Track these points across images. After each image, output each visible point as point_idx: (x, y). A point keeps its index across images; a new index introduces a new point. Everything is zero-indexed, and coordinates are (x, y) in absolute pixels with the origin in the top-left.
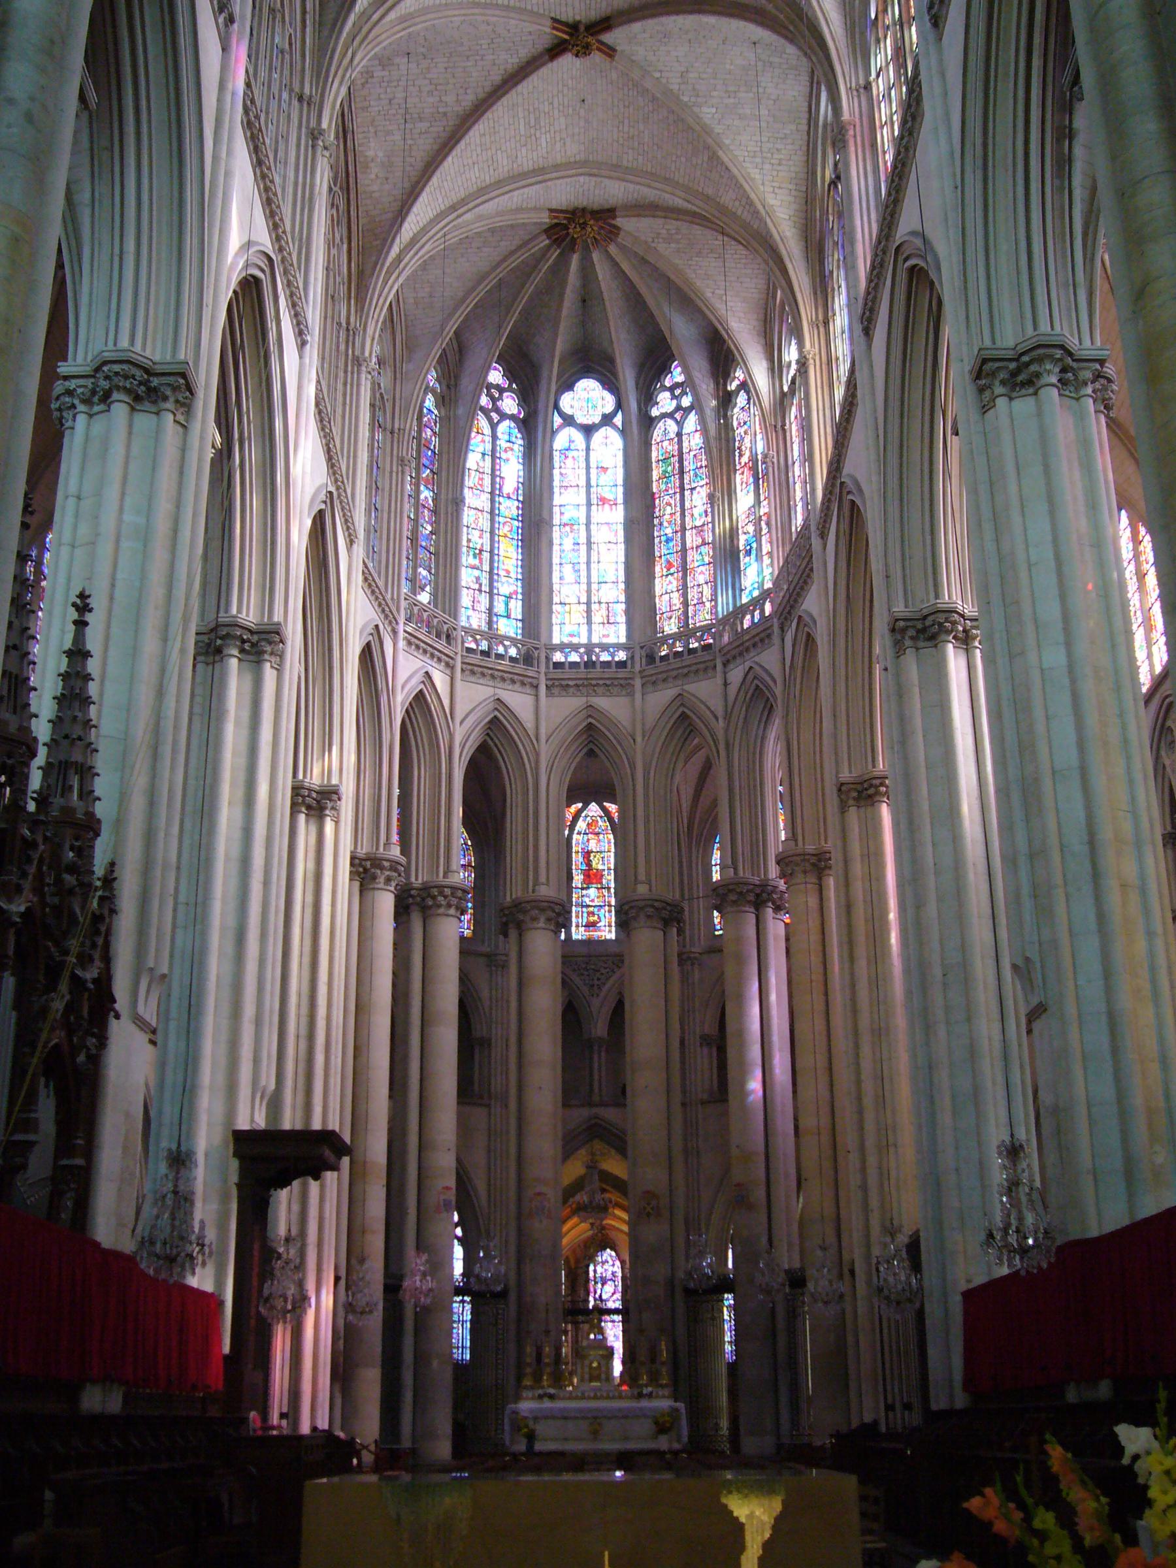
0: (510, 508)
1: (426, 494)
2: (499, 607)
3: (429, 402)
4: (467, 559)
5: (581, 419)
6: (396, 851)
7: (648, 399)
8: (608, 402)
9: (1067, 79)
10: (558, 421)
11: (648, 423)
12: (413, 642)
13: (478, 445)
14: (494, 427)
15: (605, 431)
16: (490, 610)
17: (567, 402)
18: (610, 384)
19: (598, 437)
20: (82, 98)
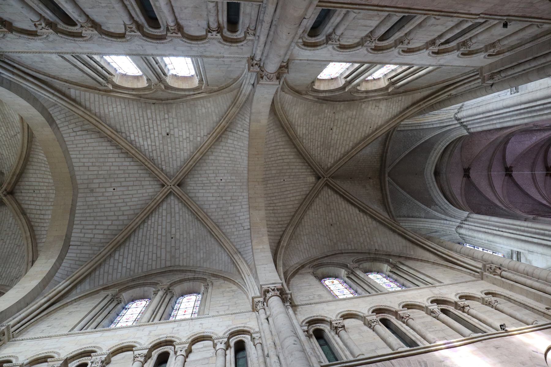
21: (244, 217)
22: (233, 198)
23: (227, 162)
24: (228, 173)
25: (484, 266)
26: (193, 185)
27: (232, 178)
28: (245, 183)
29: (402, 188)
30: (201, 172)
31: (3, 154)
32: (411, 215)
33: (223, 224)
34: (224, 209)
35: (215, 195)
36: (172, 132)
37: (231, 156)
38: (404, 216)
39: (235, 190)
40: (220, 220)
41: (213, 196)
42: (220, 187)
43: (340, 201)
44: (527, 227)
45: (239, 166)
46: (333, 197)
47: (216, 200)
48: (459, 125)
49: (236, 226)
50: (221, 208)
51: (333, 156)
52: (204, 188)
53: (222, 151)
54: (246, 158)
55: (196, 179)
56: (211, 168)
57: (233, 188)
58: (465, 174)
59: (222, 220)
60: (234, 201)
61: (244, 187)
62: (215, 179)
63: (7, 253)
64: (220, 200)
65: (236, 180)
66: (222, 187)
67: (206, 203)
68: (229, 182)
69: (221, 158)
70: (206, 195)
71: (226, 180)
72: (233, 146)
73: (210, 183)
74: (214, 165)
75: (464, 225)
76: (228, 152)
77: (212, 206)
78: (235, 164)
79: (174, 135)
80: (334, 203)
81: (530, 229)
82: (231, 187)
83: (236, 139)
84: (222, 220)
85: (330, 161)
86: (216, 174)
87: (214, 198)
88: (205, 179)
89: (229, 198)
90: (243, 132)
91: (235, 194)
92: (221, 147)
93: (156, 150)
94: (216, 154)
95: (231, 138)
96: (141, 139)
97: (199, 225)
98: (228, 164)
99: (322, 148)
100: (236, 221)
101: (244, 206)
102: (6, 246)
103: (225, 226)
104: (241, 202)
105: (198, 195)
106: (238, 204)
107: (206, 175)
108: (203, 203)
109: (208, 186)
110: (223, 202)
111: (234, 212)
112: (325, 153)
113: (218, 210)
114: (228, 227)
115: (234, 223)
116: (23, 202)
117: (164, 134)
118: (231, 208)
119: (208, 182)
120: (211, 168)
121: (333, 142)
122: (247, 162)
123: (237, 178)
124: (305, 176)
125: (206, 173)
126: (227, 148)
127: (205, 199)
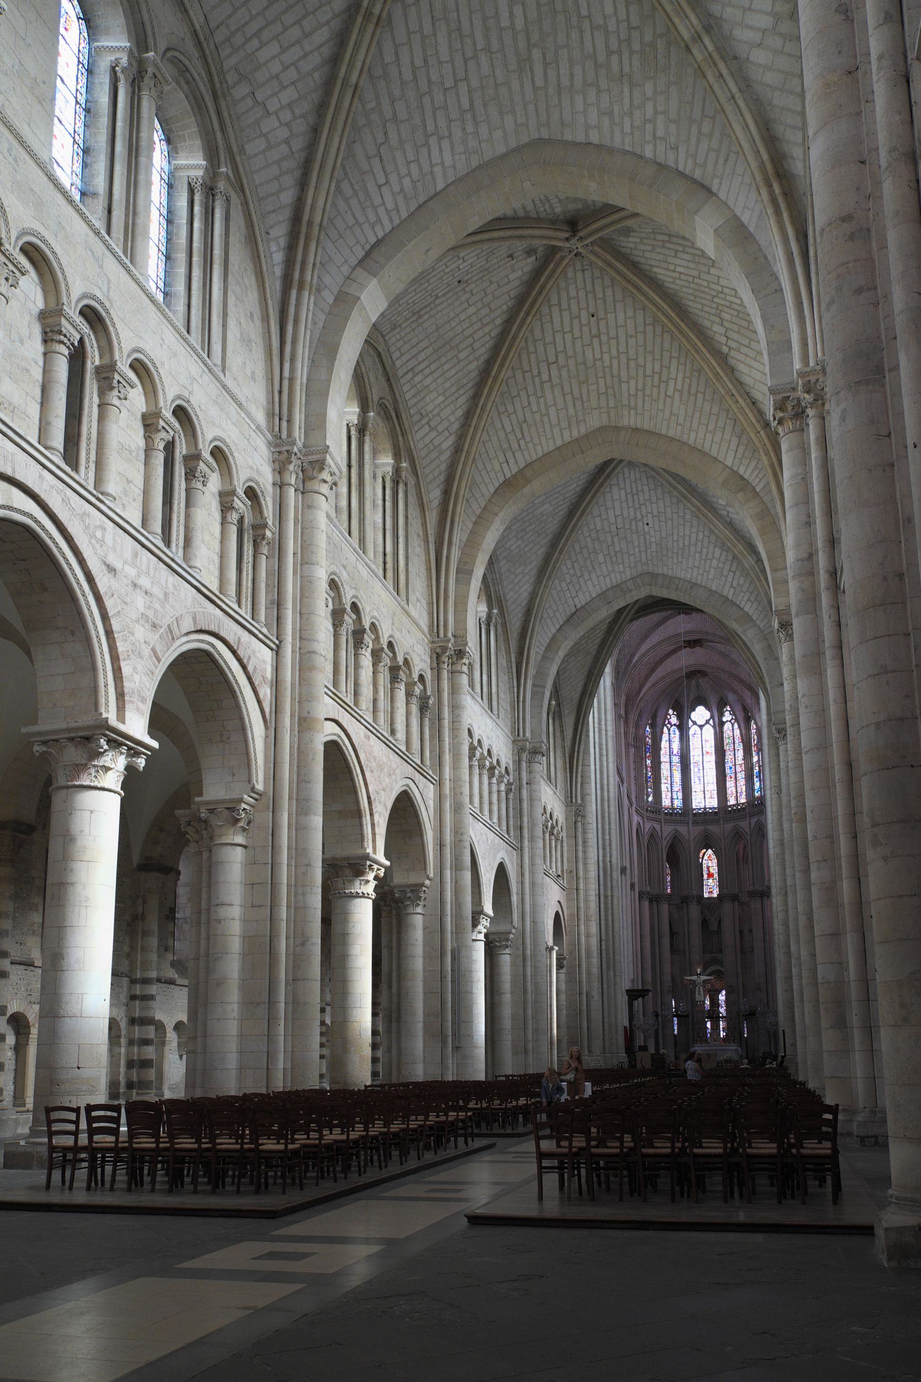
0: (676, 759)
1: (649, 762)
2: (675, 796)
3: (648, 729)
4: (663, 781)
5: (699, 723)
6: (648, 888)
7: (721, 714)
8: (707, 714)
10: (690, 723)
11: (722, 724)
12: (649, 819)
13: (665, 737)
14: (669, 730)
15: (708, 726)
16: (672, 799)
17: (694, 716)
18: (708, 707)
19: (704, 728)
21: (591, 588)
22: (619, 555)
23: (681, 539)
24: (661, 538)
25: (580, 805)
26: (633, 476)
27: (654, 544)
28: (645, 567)
30: (659, 491)
31: (675, 256)
33: (572, 553)
34: (597, 547)
35: (619, 520)
37: (692, 549)
39: (631, 553)
40: (577, 546)
41: (616, 517)
42: (634, 523)
44: (606, 731)
45: (675, 561)
47: (610, 525)
49: (575, 580)
50: (598, 539)
52: (629, 496)
53: (701, 535)
54: (688, 577)
55: (645, 482)
56: (668, 510)
57: (634, 547)
59: (578, 550)
60: (614, 559)
61: (640, 569)
62: (648, 513)
63: (451, 334)
64: (610, 532)
65: (649, 551)
66: (634, 528)
67: (603, 508)
68: (645, 539)
69: (687, 532)
70: (617, 504)
71: (649, 533)
72: (710, 557)
73: (640, 505)
74: (675, 516)
76: (699, 544)
77: (598, 520)
78: (677, 553)
81: (604, 737)
82: (636, 543)
83: (721, 565)
84: (578, 550)
86: (659, 516)
87: (612, 520)
88: (647, 497)
89: (618, 549)
90: (732, 586)
91: (626, 556)
92: (706, 533)
94: (695, 522)
95: (723, 558)
97: (560, 513)
98: (678, 541)
100: (582, 576)
101: (607, 579)
102: (462, 316)
103: (570, 558)
104: (613, 571)
105: (615, 490)
106: (610, 569)
107: (654, 500)
108: (601, 503)
109: (633, 501)
110: (609, 539)
111: (596, 567)
113: (594, 535)
114: (570, 566)
115: (579, 574)
116: (563, 284)
118: (601, 558)
119: (642, 501)
120: (668, 510)
122: (682, 577)
123: (654, 554)
125: (658, 499)
126: (706, 545)
127: (609, 505)
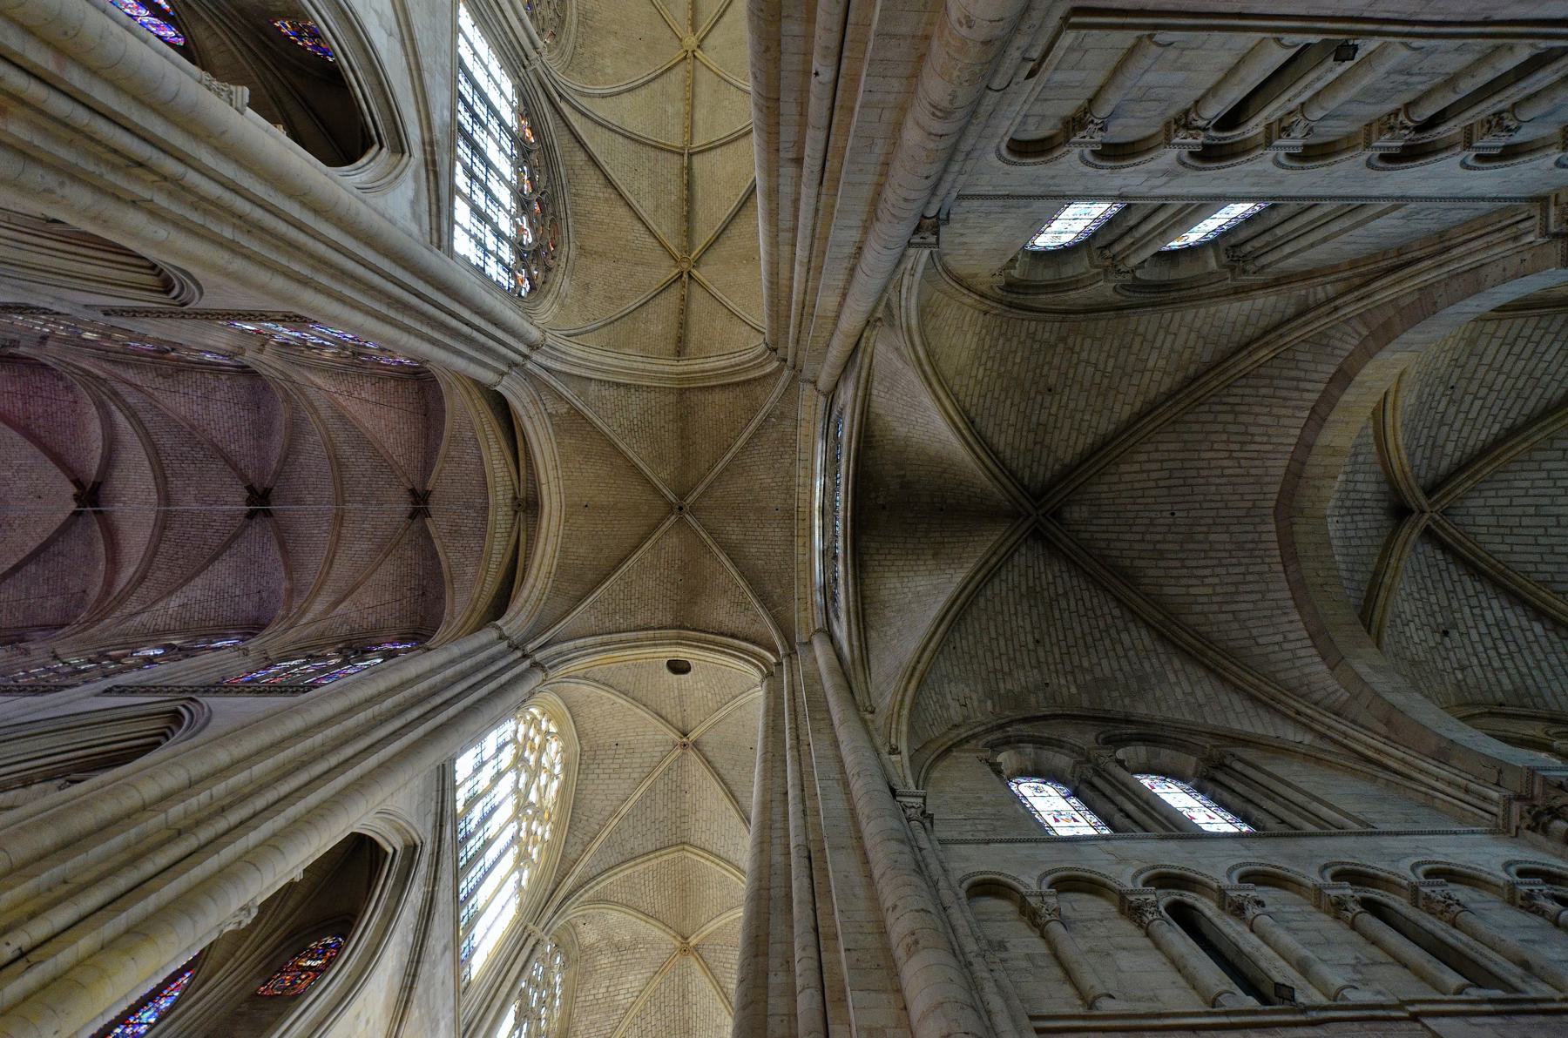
9: (75, 776)
20: (55, 221)
29: (634, 466)
32: (622, 391)
36: (1438, 637)
38: (638, 388)
43: (1008, 451)
46: (1021, 465)
48: (530, 647)
51: (1016, 569)
58: (426, 502)
75: (523, 349)
79: (1434, 632)
80: (1022, 447)
85: (1023, 558)
93: (1468, 597)
96: (1513, 622)
99: (1052, 590)
112: (1039, 578)
117: (1454, 634)
121: (1026, 608)
124: (1094, 522)
